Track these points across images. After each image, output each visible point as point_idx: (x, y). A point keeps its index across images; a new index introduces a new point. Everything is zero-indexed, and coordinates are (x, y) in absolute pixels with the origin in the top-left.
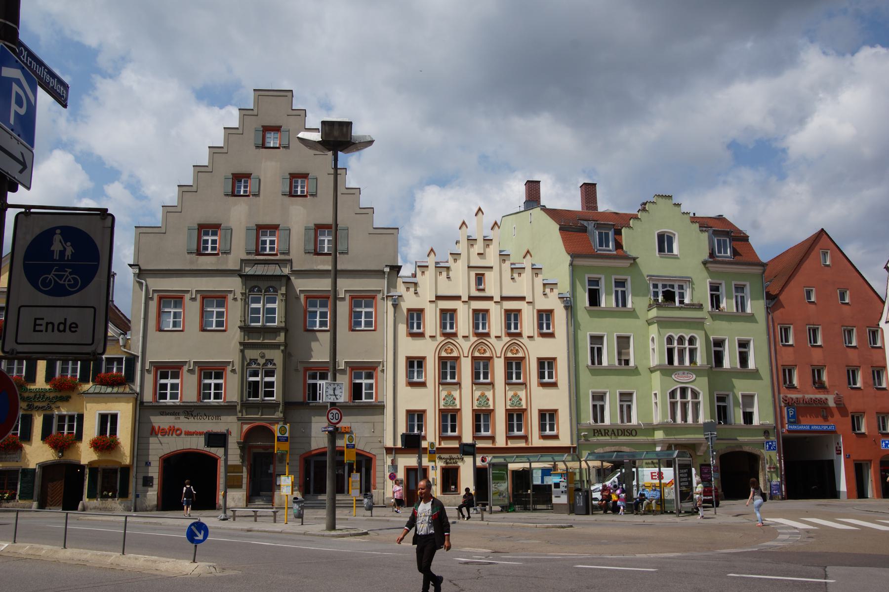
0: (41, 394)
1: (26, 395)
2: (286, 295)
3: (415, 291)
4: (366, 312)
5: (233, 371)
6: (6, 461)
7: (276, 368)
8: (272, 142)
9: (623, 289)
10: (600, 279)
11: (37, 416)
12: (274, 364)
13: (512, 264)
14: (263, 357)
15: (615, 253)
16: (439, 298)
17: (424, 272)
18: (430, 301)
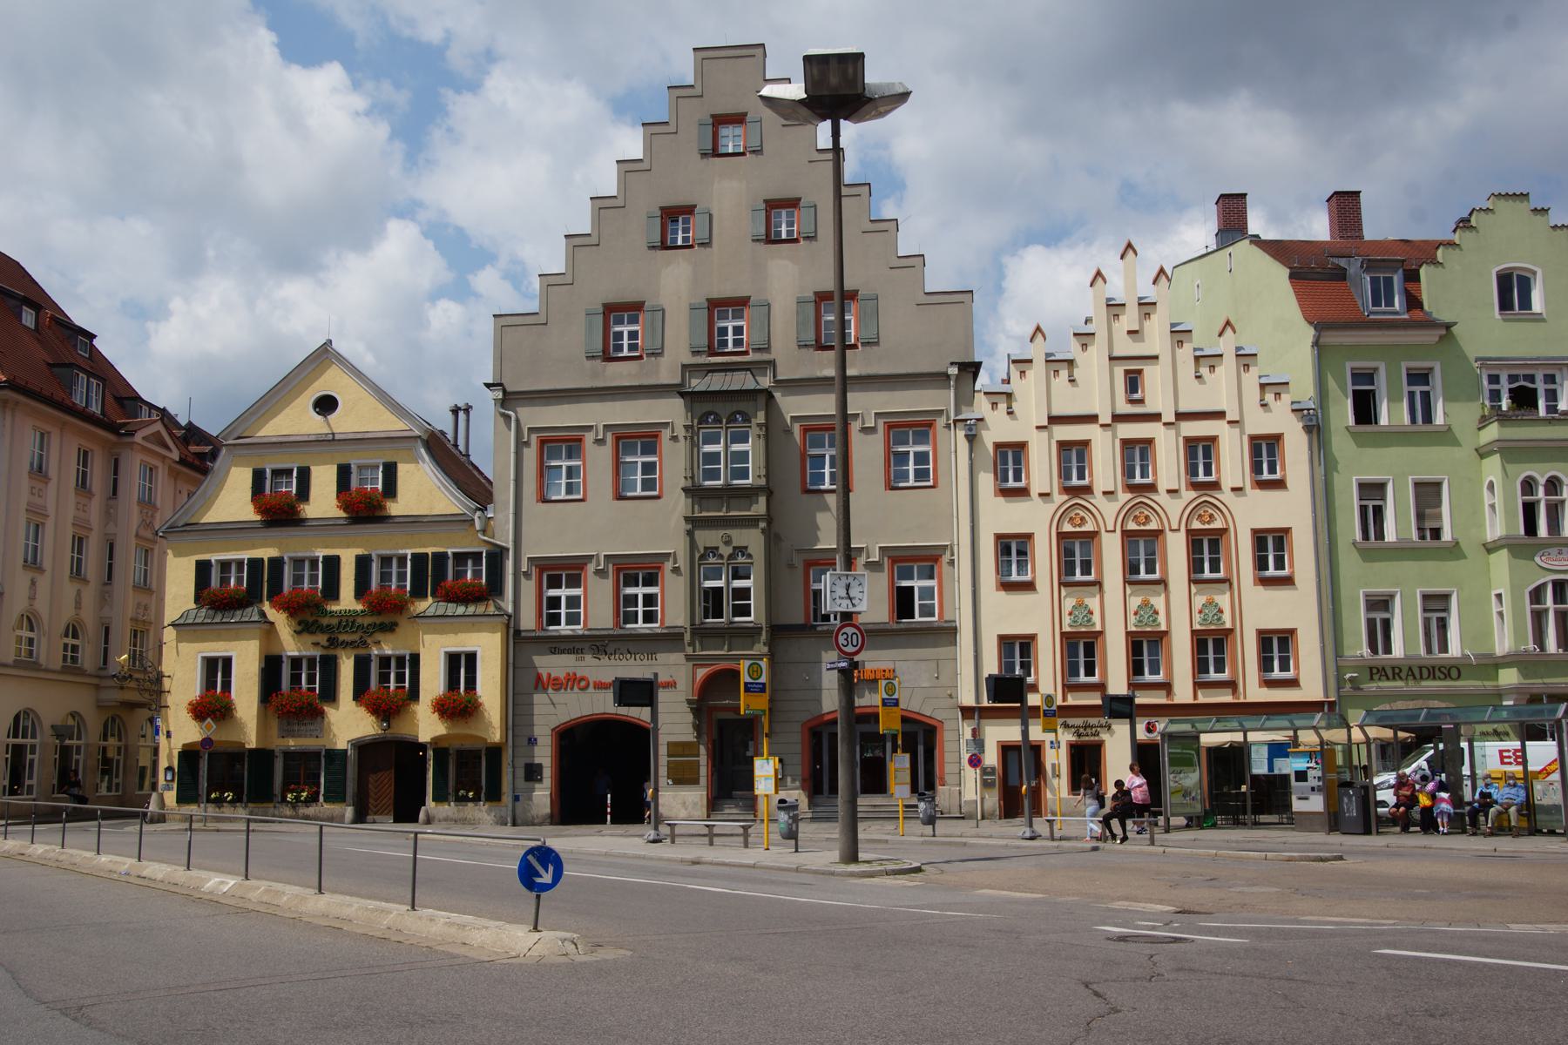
0: (348, 620)
1: (325, 621)
2: (766, 426)
3: (1008, 408)
4: (916, 454)
5: (676, 570)
6: (300, 736)
7: (752, 563)
8: (731, 145)
10: (1376, 369)
11: (344, 658)
12: (750, 556)
13: (1195, 350)
14: (728, 542)
15: (1406, 316)
16: (1054, 420)
17: (1024, 372)
18: (1038, 428)
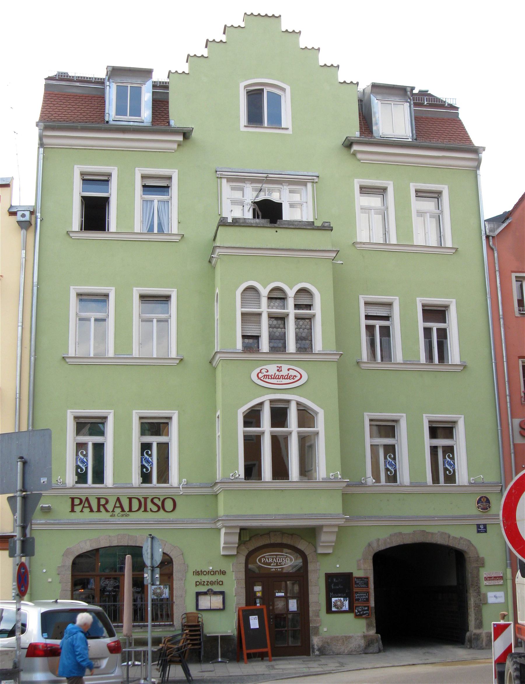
9: (441, 325)
